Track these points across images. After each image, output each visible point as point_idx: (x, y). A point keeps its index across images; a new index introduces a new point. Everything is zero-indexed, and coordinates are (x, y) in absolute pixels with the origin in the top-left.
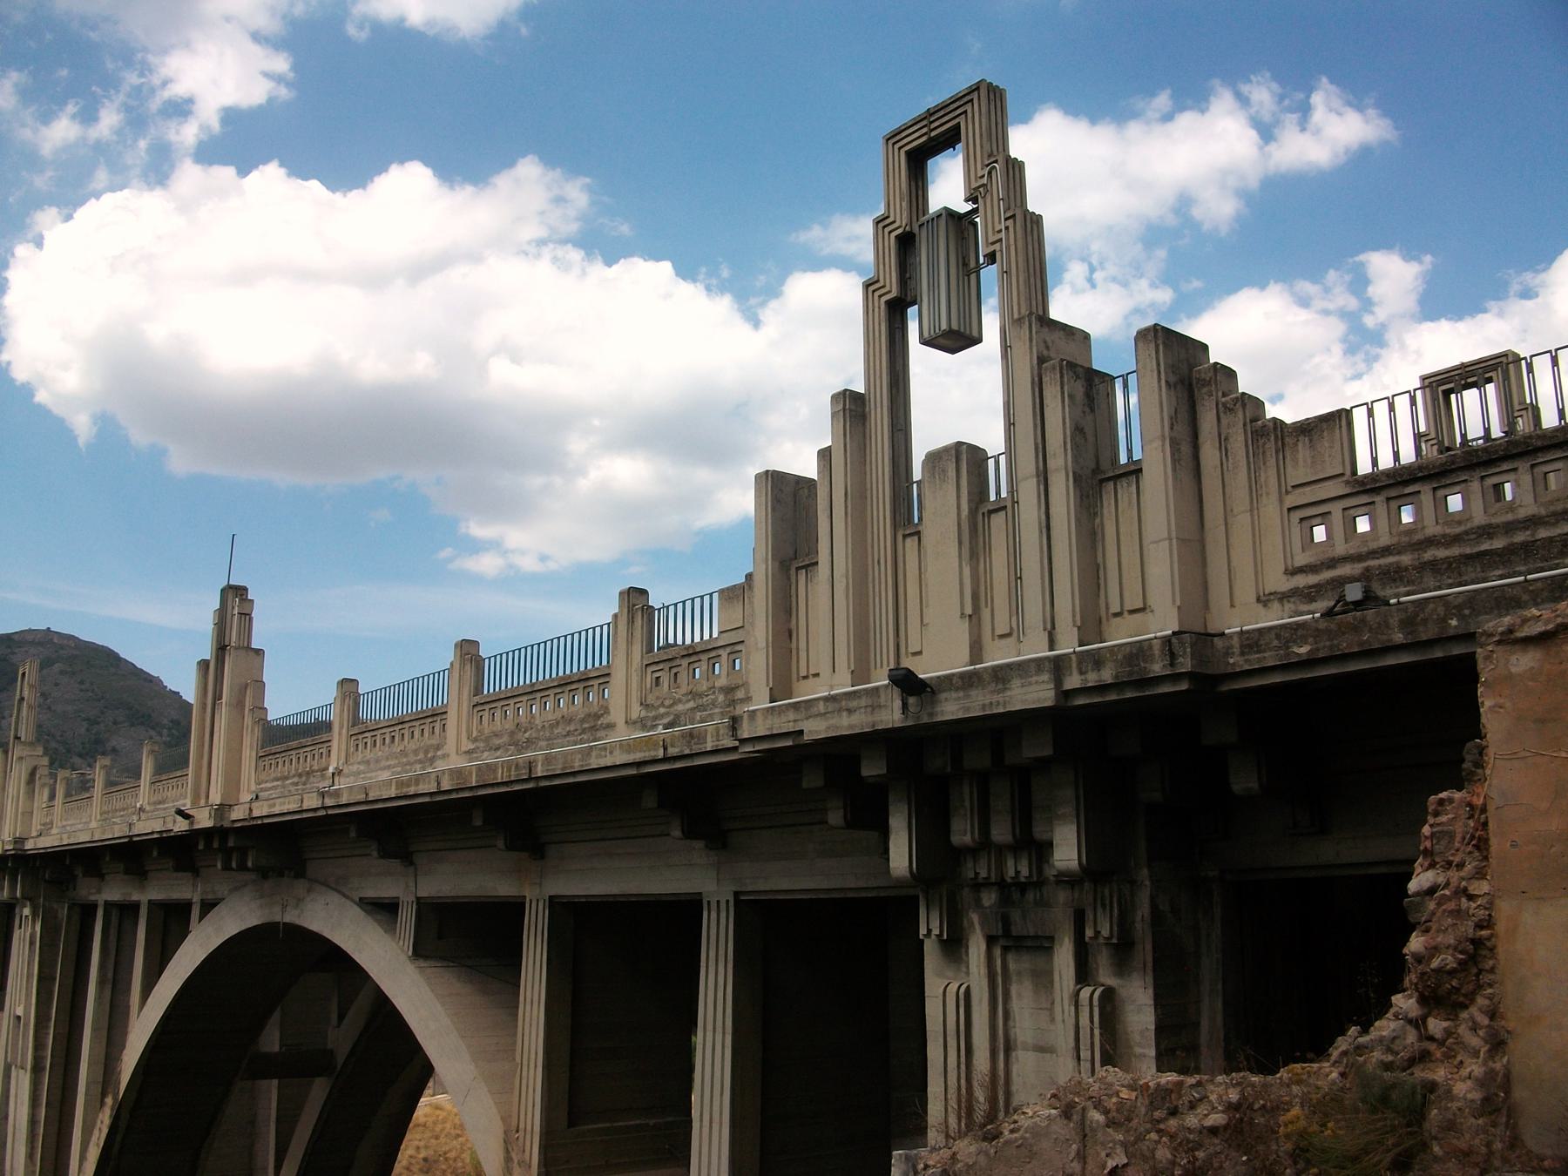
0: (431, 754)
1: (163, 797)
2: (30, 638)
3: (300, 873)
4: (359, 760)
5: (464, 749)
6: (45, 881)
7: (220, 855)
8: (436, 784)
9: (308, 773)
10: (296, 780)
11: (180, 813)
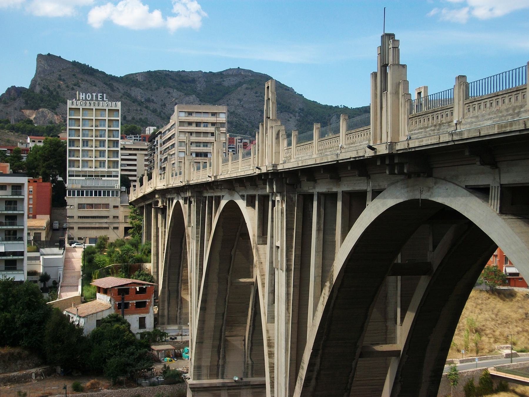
0: (516, 111)
1: (353, 141)
2: (231, 73)
4: (471, 116)
6: (287, 184)
8: (524, 125)
9: (440, 125)
10: (433, 128)
11: (370, 147)
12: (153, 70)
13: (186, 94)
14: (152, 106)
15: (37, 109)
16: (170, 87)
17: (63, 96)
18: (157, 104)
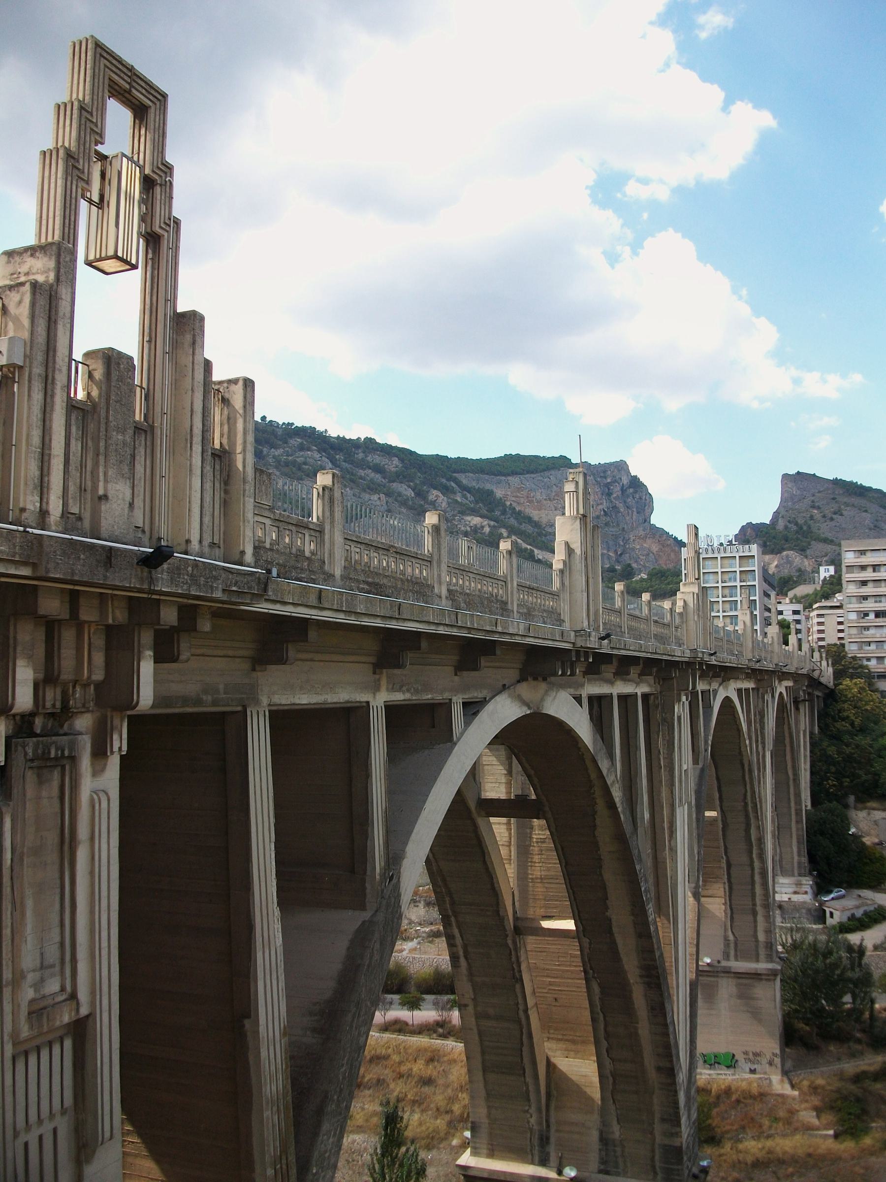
15: (780, 553)
17: (817, 531)
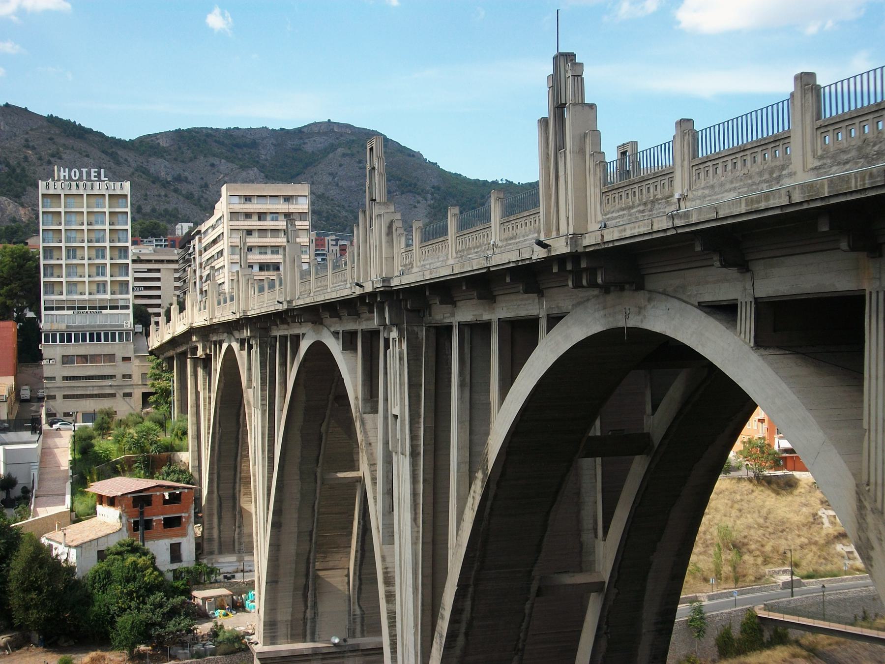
0: (776, 173)
1: (513, 234)
2: (316, 130)
3: (639, 285)
4: (702, 185)
5: (810, 166)
6: (407, 310)
7: (570, 277)
8: (788, 198)
9: (653, 202)
10: (641, 208)
11: (540, 243)
12: (185, 128)
13: (241, 167)
14: (184, 188)
16: (214, 155)
17: (33, 175)
18: (193, 184)
